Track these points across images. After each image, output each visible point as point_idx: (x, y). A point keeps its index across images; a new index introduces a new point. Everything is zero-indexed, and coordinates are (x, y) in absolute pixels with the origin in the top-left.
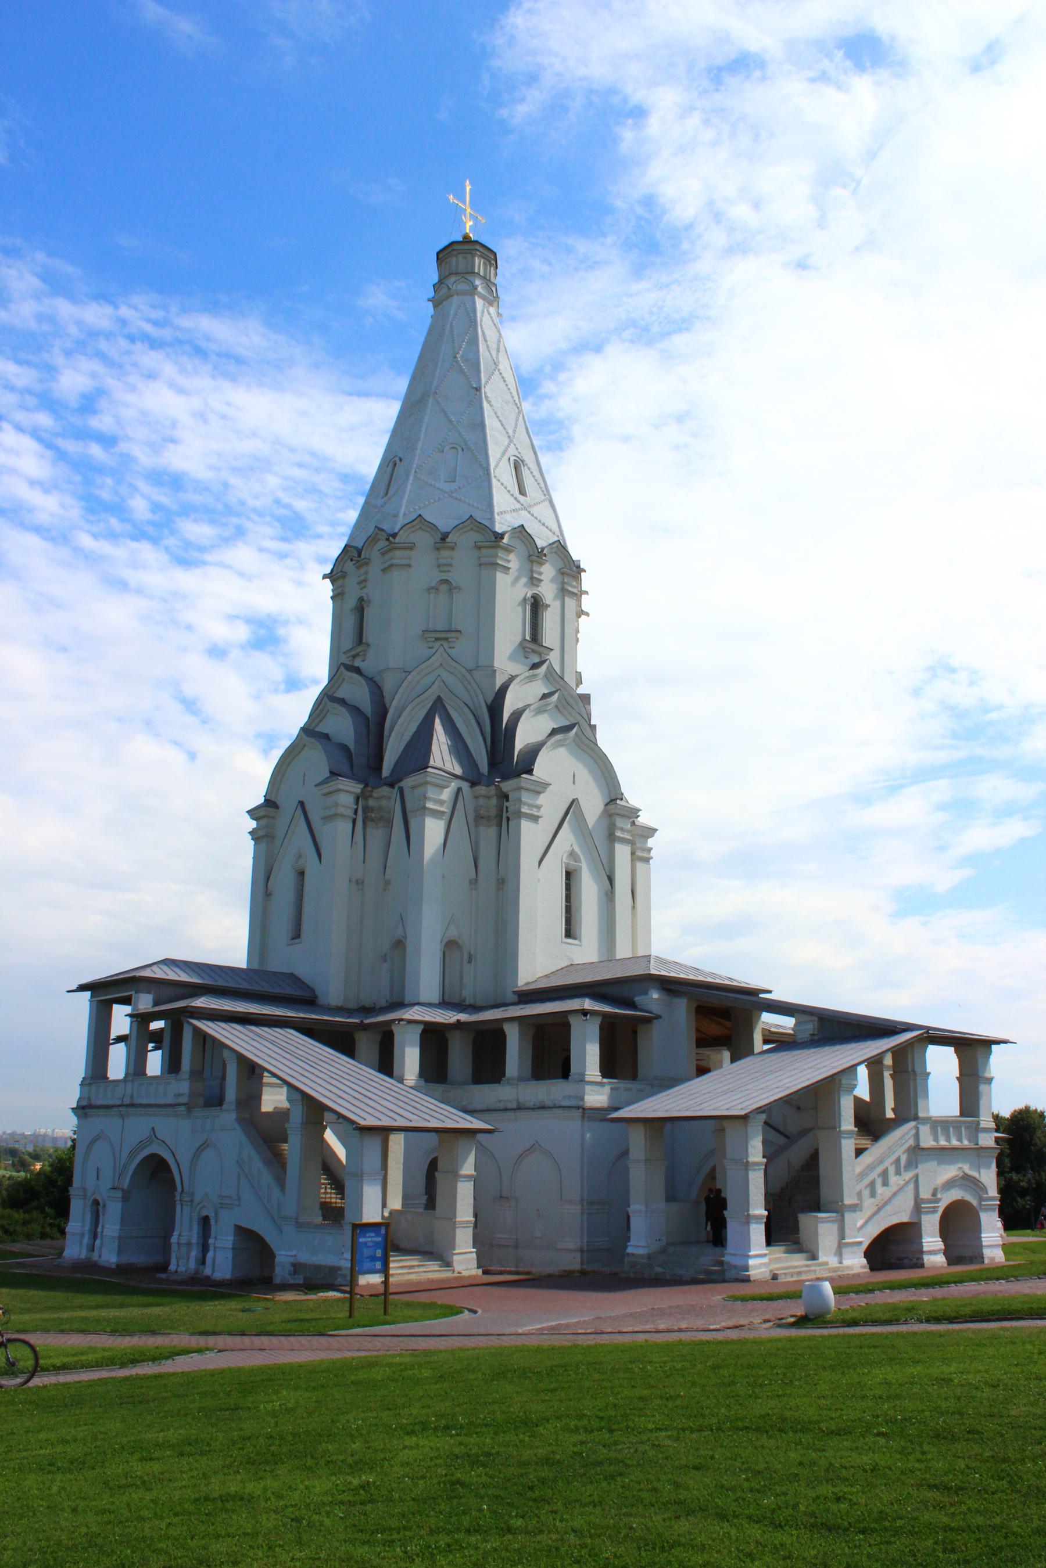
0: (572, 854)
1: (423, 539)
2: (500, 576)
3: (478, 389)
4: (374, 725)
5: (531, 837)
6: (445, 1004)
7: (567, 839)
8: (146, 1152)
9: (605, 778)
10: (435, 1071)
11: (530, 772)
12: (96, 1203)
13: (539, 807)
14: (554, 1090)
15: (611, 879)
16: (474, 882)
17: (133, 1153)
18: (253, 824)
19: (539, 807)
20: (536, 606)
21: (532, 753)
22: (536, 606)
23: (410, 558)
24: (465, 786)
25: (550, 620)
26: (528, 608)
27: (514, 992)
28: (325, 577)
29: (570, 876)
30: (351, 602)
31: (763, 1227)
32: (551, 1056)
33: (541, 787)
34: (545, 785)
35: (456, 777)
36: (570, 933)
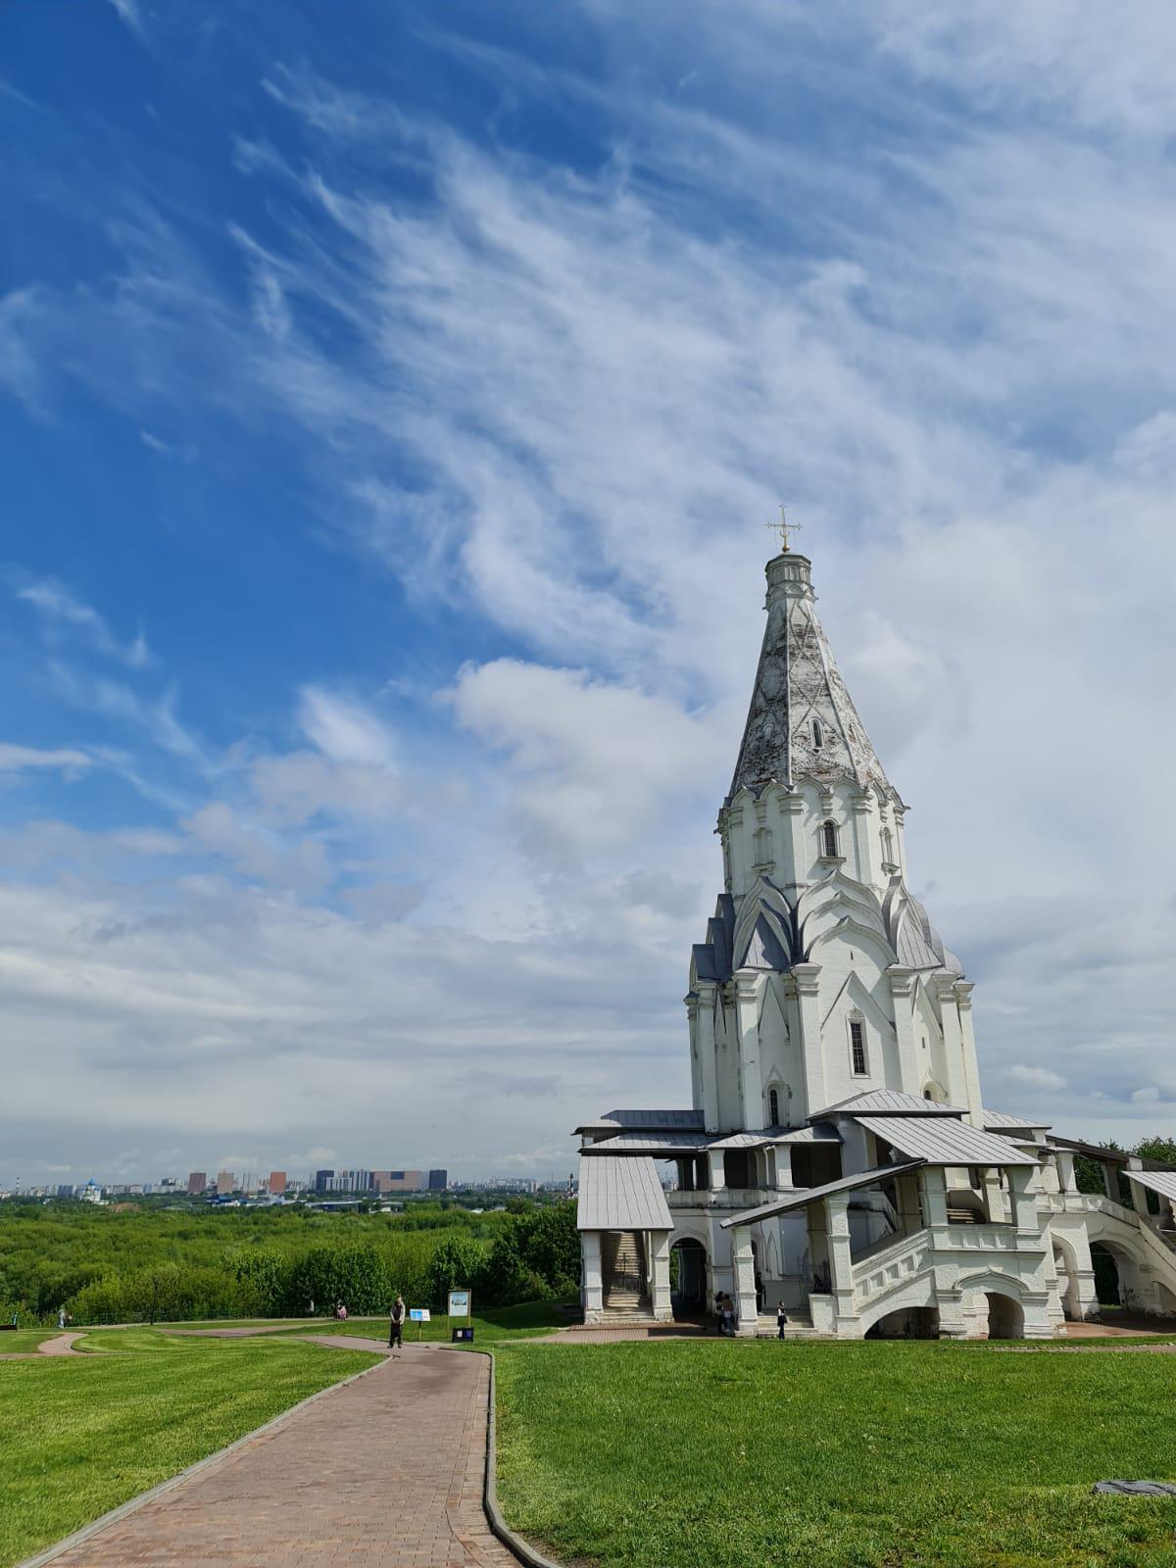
1: (746, 801)
5: (812, 1009)
7: (847, 1004)
9: (882, 950)
11: (806, 961)
13: (816, 985)
15: (893, 1024)
18: (688, 1008)
19: (816, 985)
20: (830, 828)
22: (830, 828)
23: (741, 817)
24: (774, 975)
25: (844, 839)
26: (823, 833)
27: (807, 1120)
28: (715, 832)
29: (857, 1029)
31: (755, 1300)
33: (816, 971)
35: (764, 970)
36: (860, 1067)
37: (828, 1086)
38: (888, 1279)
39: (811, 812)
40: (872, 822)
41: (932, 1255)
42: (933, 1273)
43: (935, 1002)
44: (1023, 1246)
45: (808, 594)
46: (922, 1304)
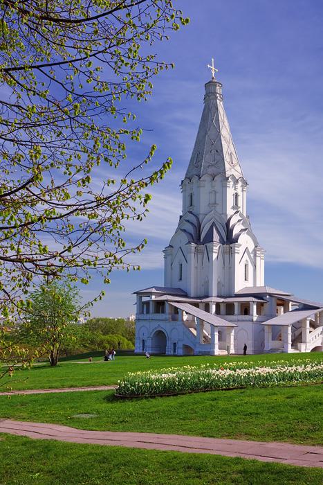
0: (247, 260)
2: (228, 189)
3: (219, 132)
4: (198, 228)
5: (237, 257)
6: (218, 296)
8: (157, 329)
10: (218, 312)
12: (144, 341)
14: (247, 317)
16: (224, 268)
17: (153, 330)
21: (238, 236)
22: (236, 196)
25: (240, 199)
30: (188, 194)
32: (246, 310)
34: (241, 245)
37: (240, 285)
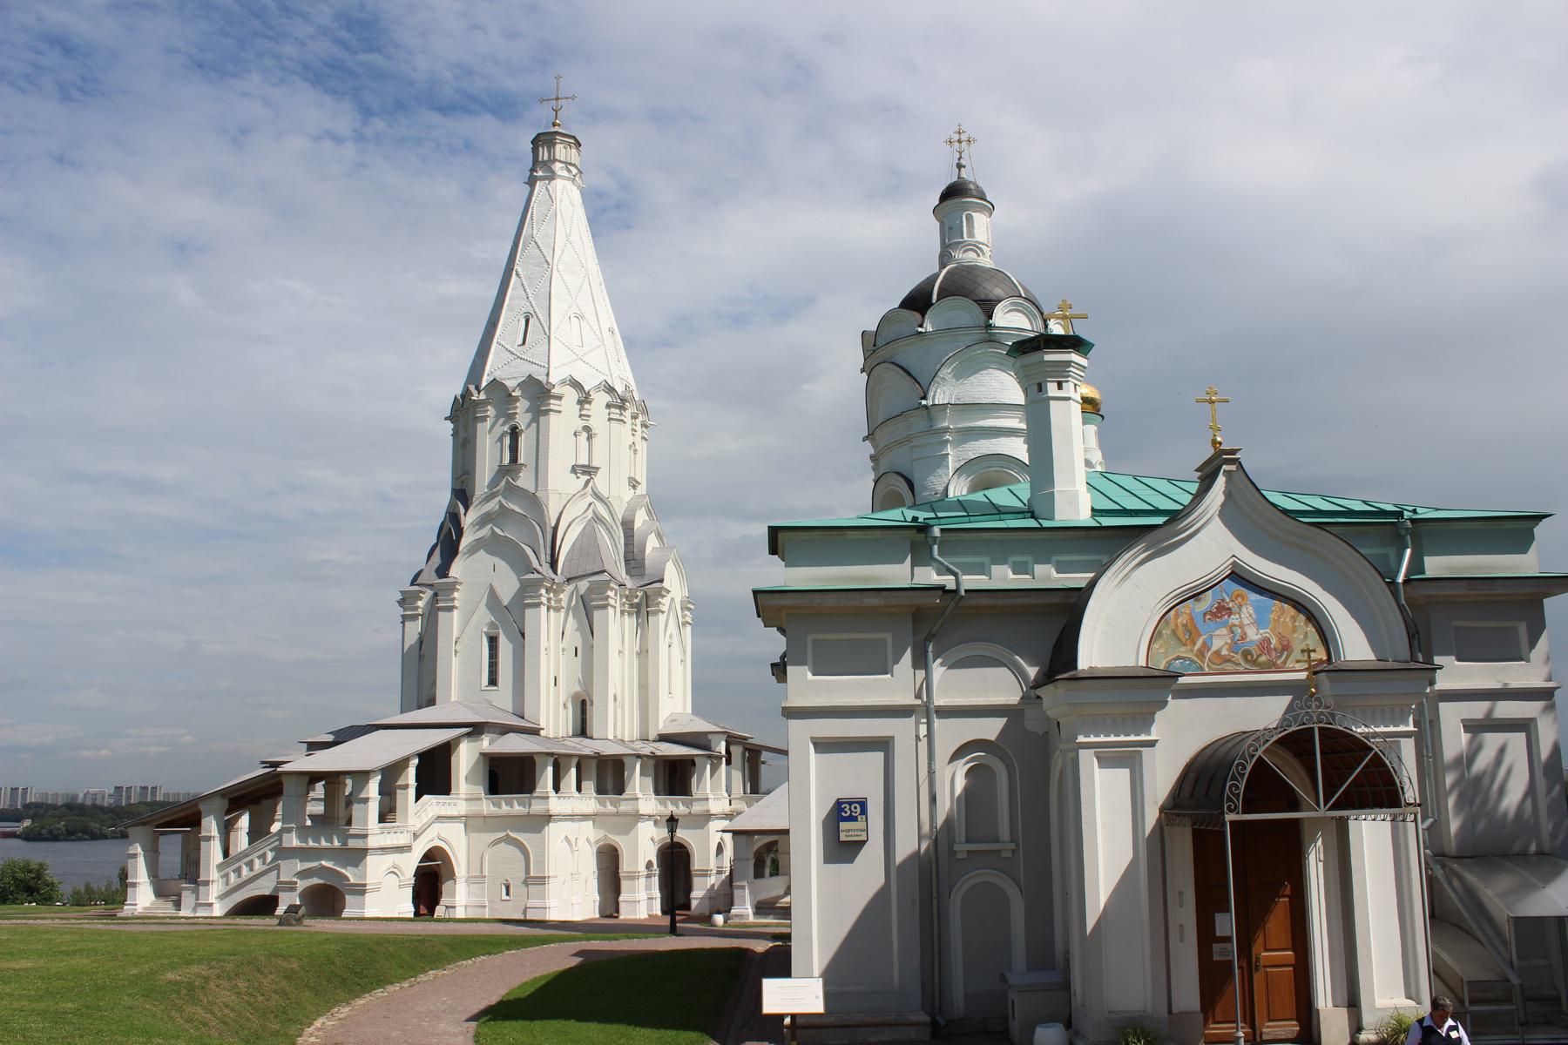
7: (483, 616)
11: (446, 576)
15: (523, 635)
22: (515, 433)
29: (493, 641)
33: (452, 587)
36: (493, 681)
38: (245, 871)
39: (497, 418)
40: (562, 421)
41: (283, 853)
42: (278, 868)
43: (588, 608)
44: (352, 843)
45: (565, 173)
46: (267, 892)
